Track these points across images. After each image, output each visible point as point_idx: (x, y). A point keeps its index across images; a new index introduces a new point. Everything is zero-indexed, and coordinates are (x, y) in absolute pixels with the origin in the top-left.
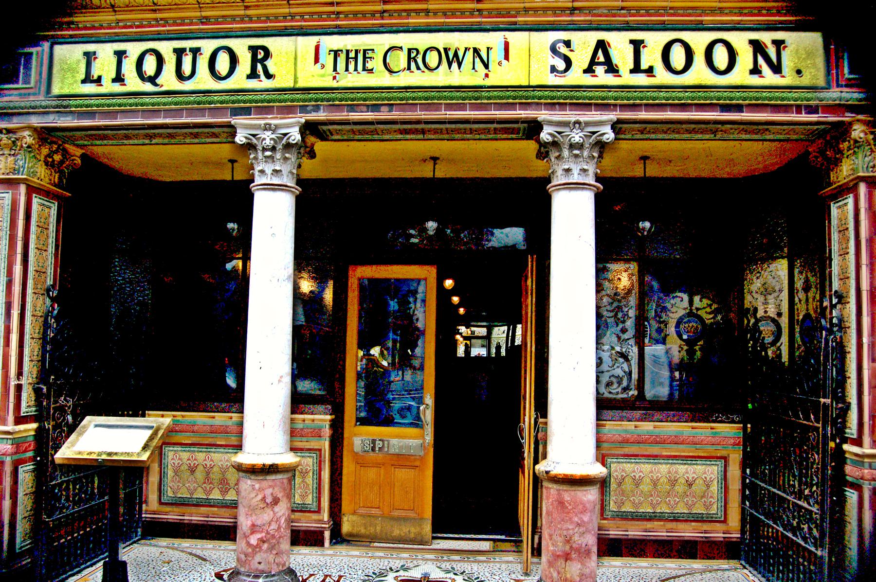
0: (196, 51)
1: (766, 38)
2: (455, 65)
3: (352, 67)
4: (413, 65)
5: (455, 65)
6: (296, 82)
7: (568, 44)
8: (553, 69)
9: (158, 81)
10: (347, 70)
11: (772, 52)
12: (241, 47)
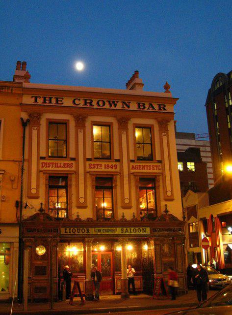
0: (80, 229)
1: (144, 228)
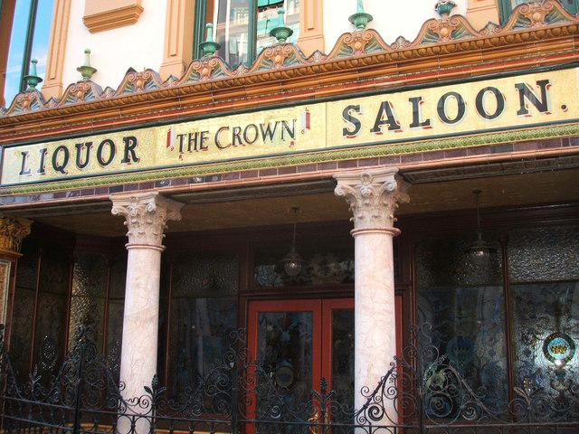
0: (89, 145)
1: (530, 80)
2: (268, 137)
3: (192, 147)
4: (237, 140)
5: (268, 137)
7: (357, 108)
8: (346, 132)
10: (189, 150)
12: (118, 138)
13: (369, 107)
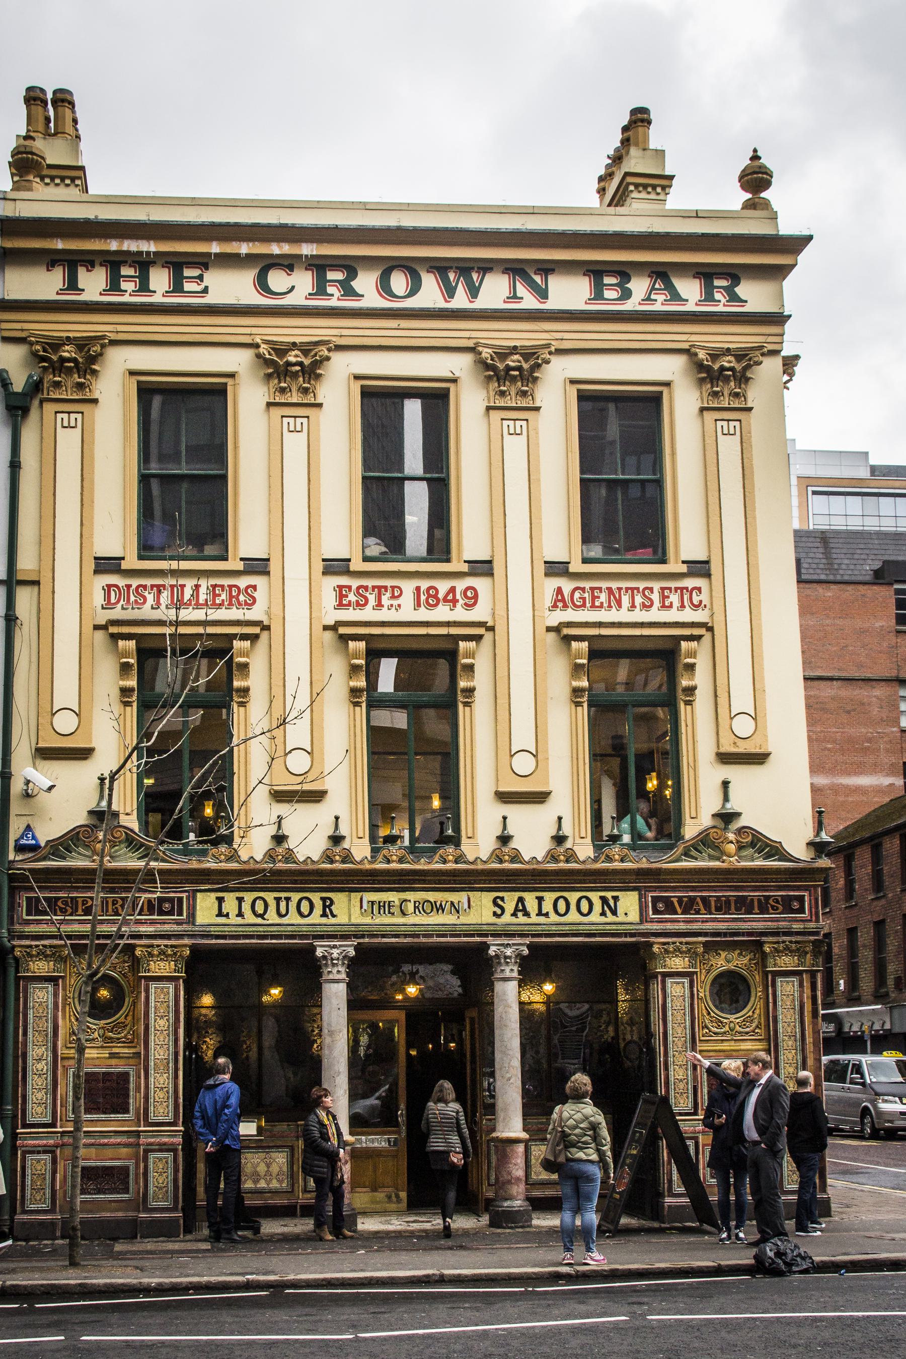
0: (288, 899)
1: (609, 895)
3: (382, 911)
5: (440, 911)
6: (350, 919)
9: (265, 917)
11: (612, 903)
12: (316, 898)
13: (510, 900)
